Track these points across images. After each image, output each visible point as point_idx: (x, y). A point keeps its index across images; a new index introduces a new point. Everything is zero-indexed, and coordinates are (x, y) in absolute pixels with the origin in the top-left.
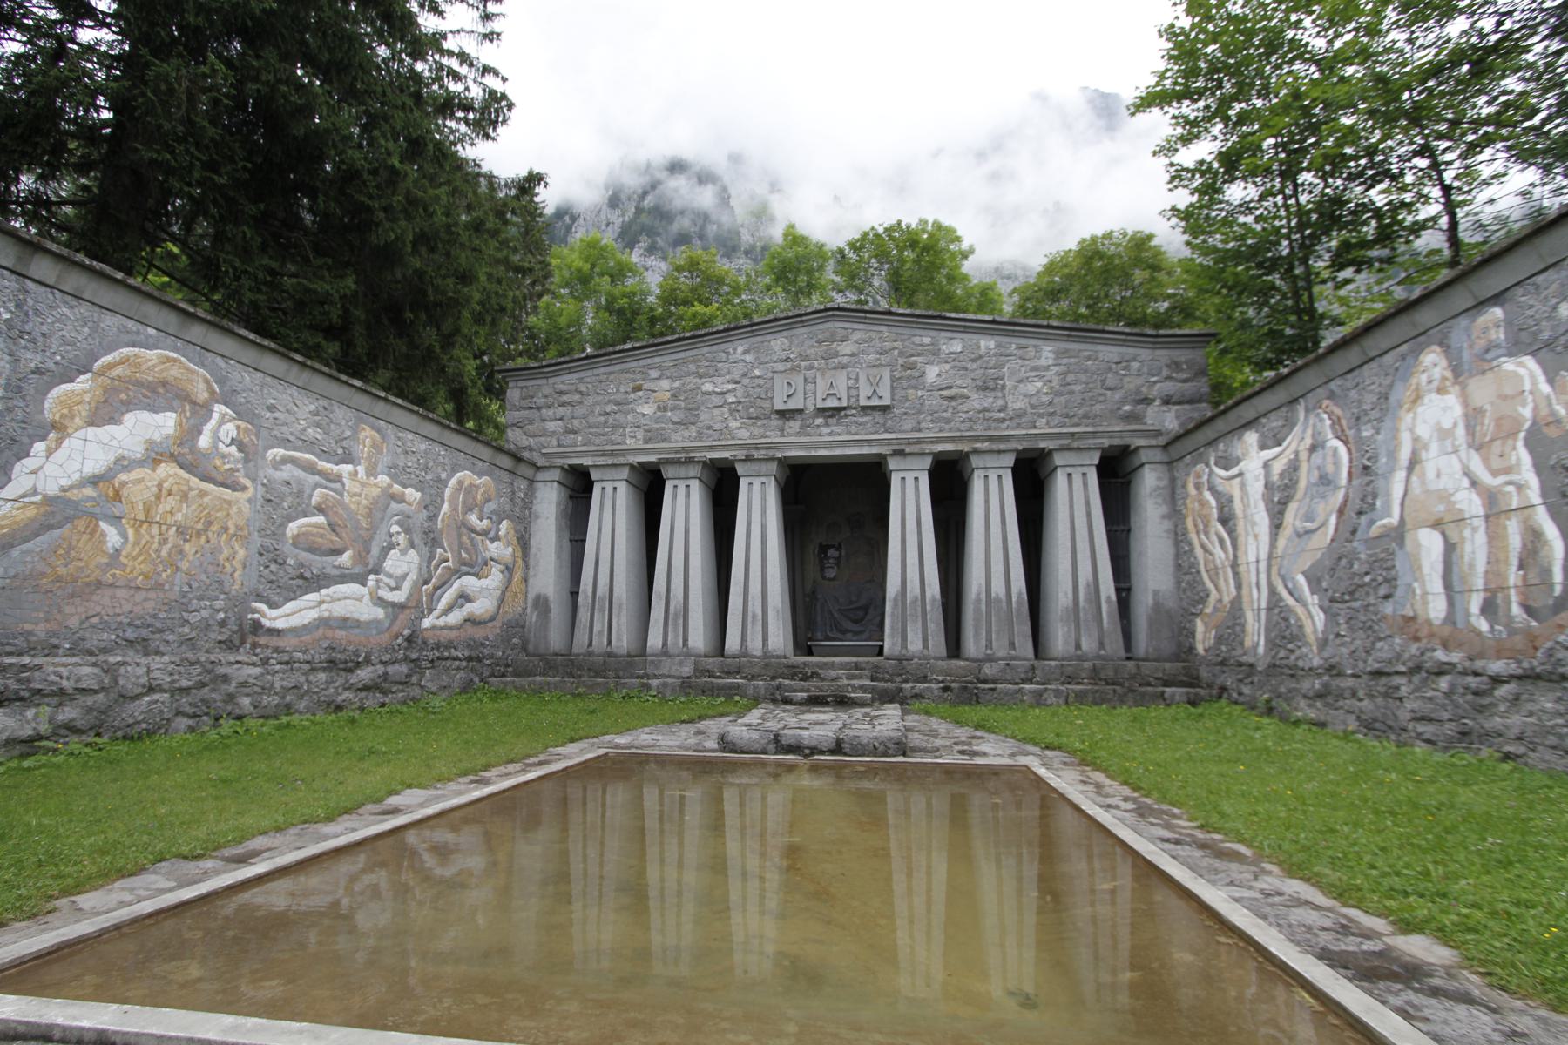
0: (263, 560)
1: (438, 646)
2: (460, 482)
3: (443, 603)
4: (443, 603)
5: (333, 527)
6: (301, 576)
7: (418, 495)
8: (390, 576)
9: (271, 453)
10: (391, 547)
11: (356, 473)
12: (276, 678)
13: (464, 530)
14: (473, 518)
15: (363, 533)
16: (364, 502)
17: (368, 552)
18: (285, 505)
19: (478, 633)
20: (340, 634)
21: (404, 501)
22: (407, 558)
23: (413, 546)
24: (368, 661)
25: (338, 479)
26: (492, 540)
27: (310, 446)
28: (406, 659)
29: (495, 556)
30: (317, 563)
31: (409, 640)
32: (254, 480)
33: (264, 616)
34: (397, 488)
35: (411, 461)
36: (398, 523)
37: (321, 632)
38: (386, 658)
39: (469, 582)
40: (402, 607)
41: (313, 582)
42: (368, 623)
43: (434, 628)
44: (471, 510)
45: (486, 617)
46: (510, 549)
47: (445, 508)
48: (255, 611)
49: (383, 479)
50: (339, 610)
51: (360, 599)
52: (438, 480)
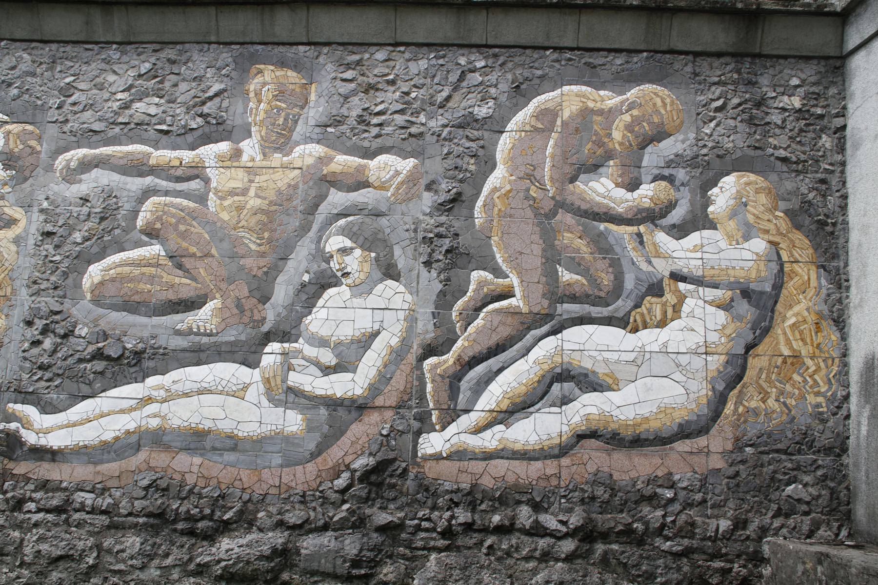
0: (33, 333)
1: (472, 497)
2: (548, 116)
3: (493, 396)
4: (493, 396)
5: (176, 259)
6: (99, 355)
7: (411, 162)
8: (323, 343)
9: (60, 162)
10: (324, 282)
11: (237, 154)
12: (32, 537)
13: (565, 218)
14: (602, 189)
15: (248, 262)
16: (253, 202)
17: (265, 299)
18: (78, 236)
19: (634, 468)
20: (187, 465)
21: (366, 184)
22: (373, 300)
23: (390, 272)
24: (245, 520)
25: (196, 172)
26: (680, 231)
27: (135, 130)
28: (358, 523)
29: (692, 265)
30: (137, 329)
31: (379, 478)
32: (27, 207)
33: (27, 425)
34: (343, 161)
35: (390, 98)
36: (344, 232)
37: (142, 455)
38: (293, 518)
39: (590, 343)
40: (358, 407)
41: (134, 363)
42: (259, 444)
43: (459, 455)
44: (594, 168)
45: (667, 424)
46: (759, 245)
47: (498, 178)
48: (10, 418)
49: (307, 153)
50: (183, 414)
51: (239, 393)
52: (468, 122)
